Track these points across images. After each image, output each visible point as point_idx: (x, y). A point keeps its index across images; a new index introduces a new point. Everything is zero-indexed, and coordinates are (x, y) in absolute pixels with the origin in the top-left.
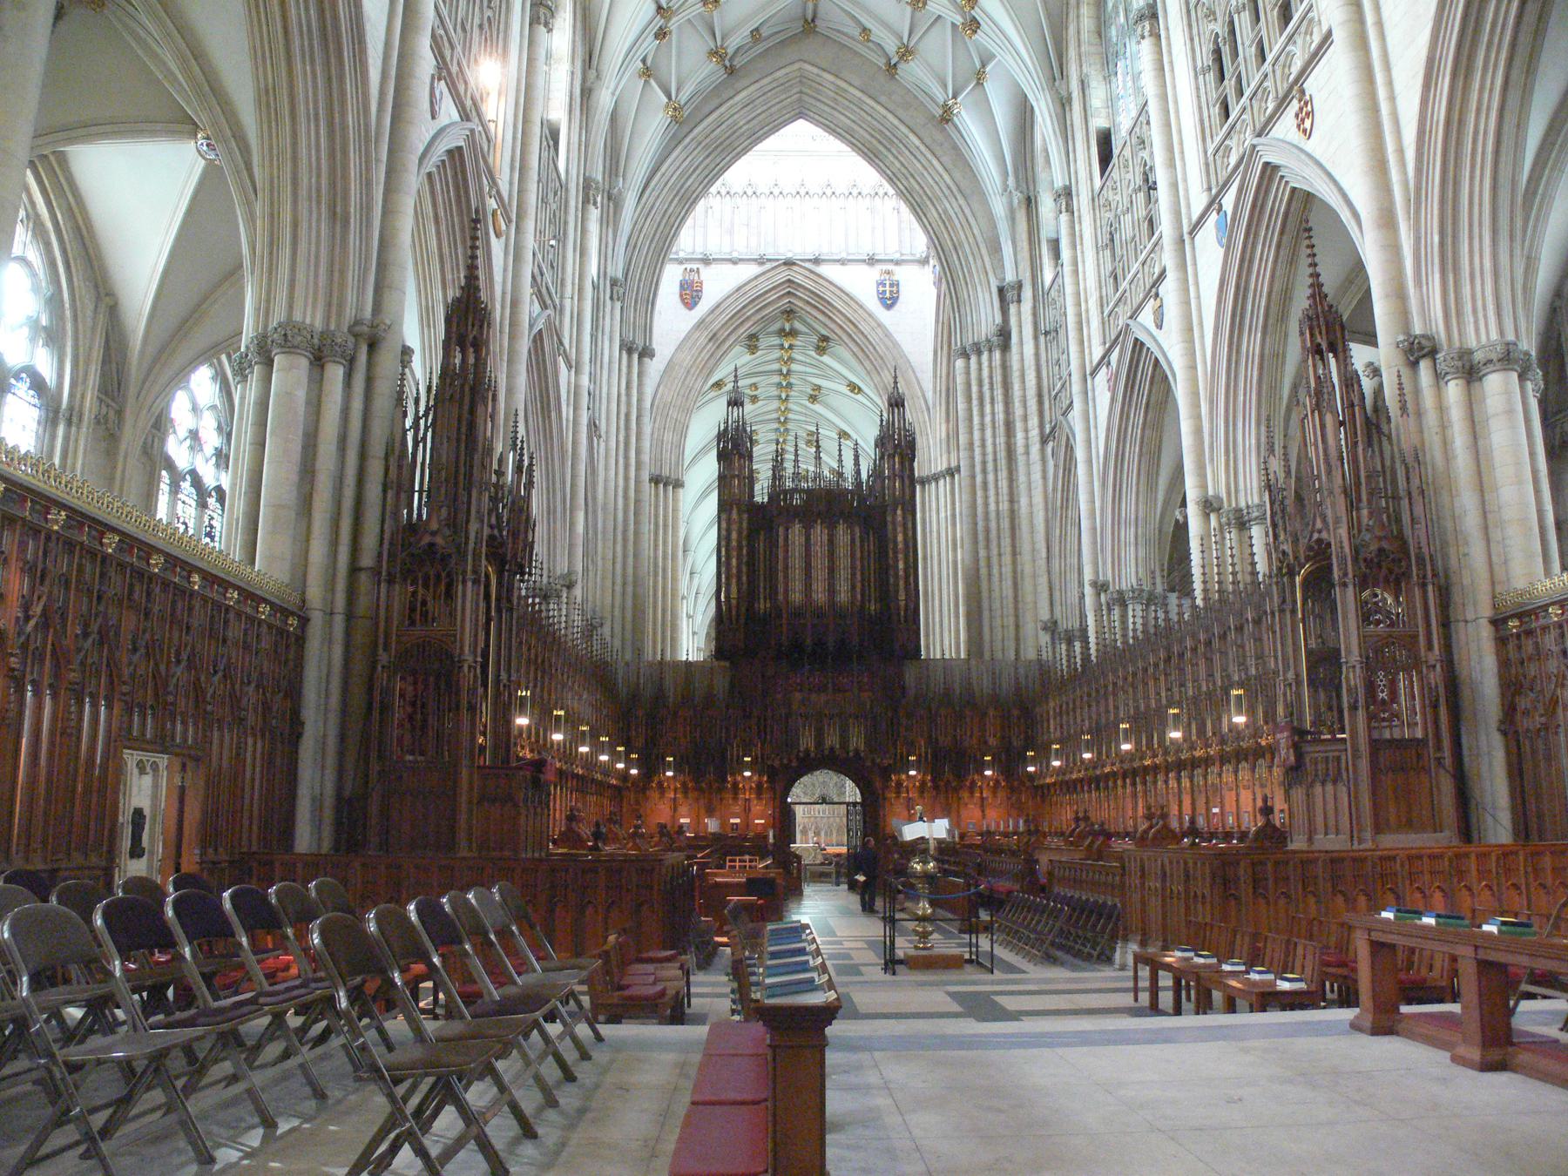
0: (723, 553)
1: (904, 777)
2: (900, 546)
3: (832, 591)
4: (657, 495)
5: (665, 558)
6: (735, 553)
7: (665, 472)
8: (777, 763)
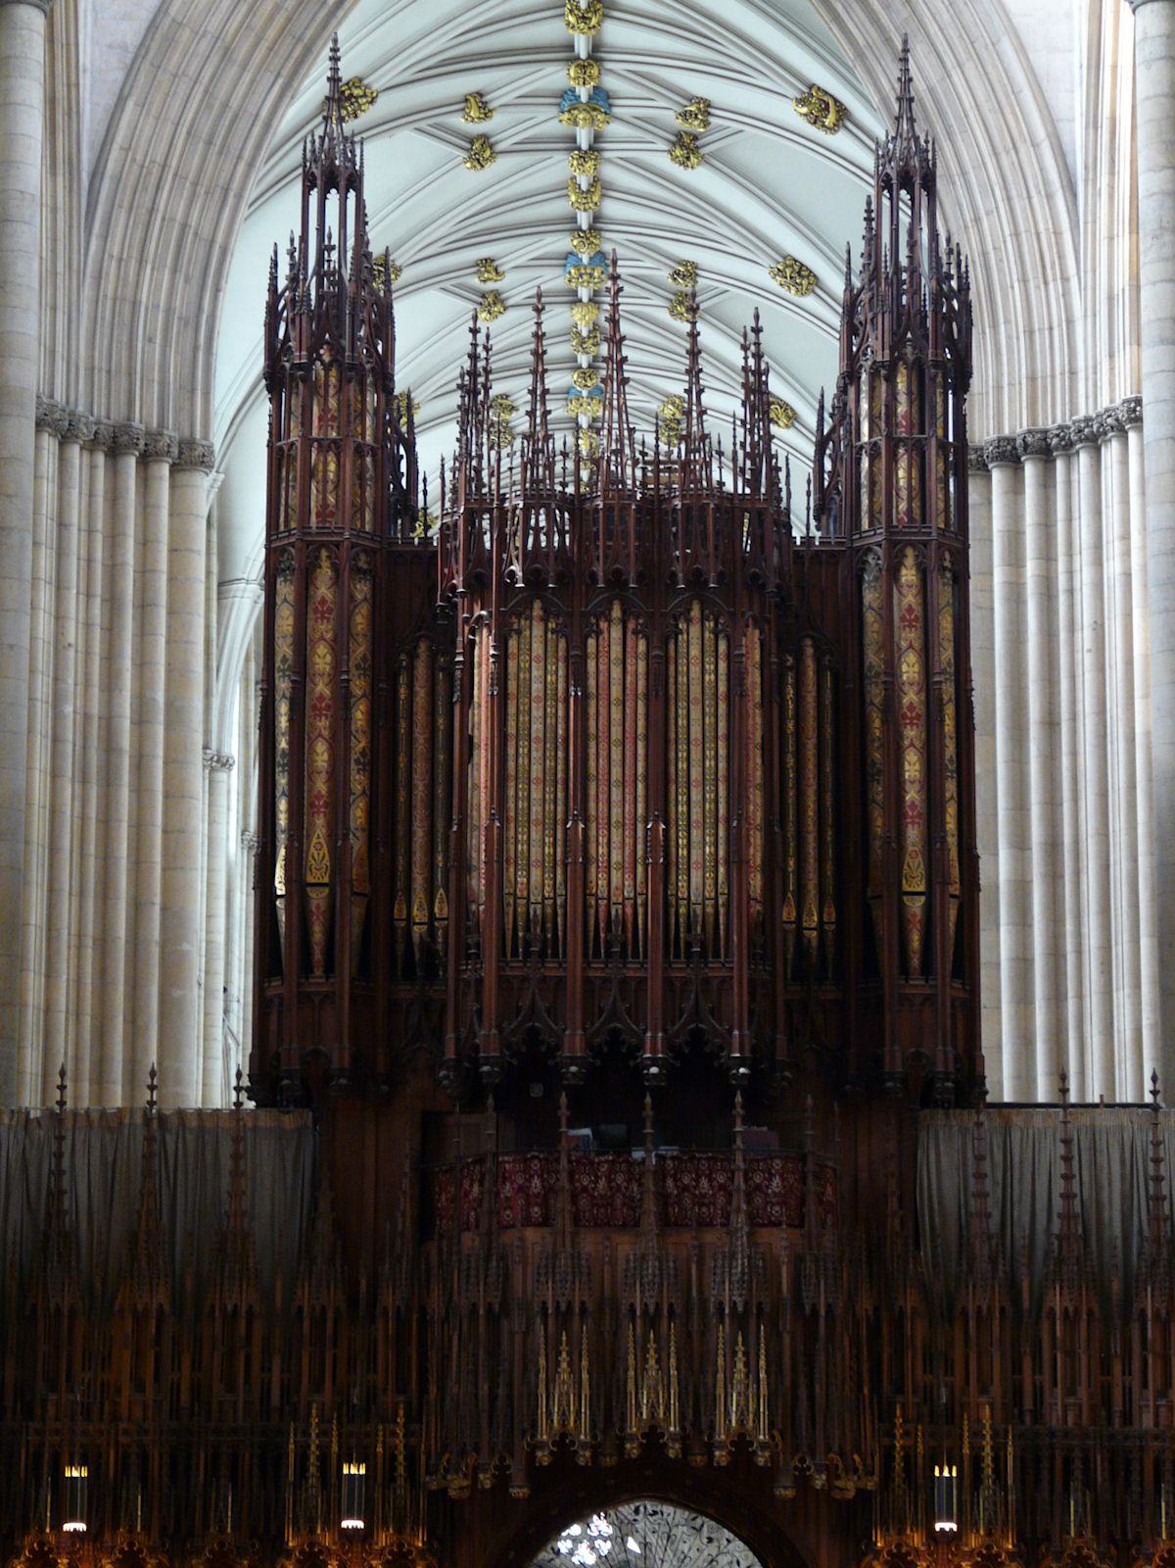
0: (283, 722)
1: (917, 1540)
2: (911, 697)
3: (663, 863)
4: (114, 498)
5: (141, 721)
6: (323, 724)
7: (145, 416)
8: (457, 1485)
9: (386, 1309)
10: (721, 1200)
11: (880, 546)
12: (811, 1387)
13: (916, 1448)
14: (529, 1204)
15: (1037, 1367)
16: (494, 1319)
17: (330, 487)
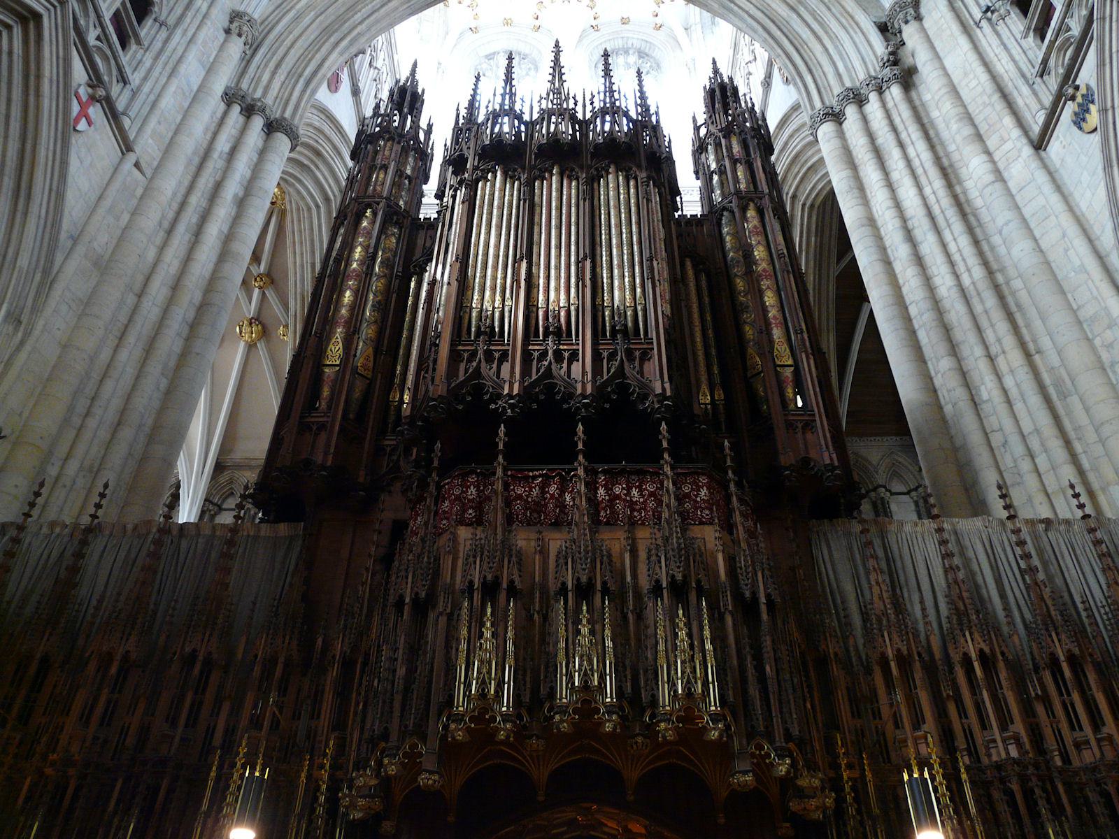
9: (334, 657)
10: (652, 504)
11: (731, 202)
12: (760, 669)
13: (863, 776)
14: (464, 511)
15: (963, 713)
16: (422, 608)
17: (379, 183)
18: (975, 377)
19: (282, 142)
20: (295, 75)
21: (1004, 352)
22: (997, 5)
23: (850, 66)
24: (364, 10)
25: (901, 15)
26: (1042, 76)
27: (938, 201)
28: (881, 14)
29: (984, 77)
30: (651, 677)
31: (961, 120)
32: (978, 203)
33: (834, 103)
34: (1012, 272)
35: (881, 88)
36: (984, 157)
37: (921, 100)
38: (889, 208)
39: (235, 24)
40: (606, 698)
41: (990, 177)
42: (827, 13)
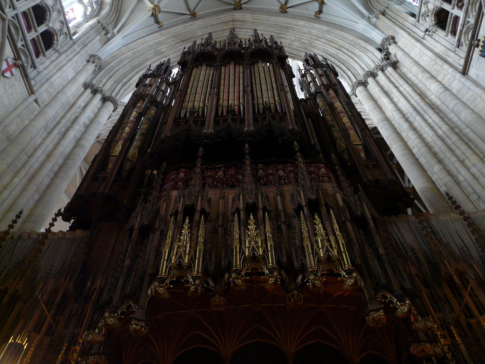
18: (454, 171)
19: (110, 106)
20: (118, 82)
21: (467, 158)
22: (430, 29)
23: (367, 64)
24: (150, 61)
25: (387, 43)
26: (458, 47)
27: (418, 104)
28: (377, 45)
29: (430, 54)
30: (300, 253)
31: (423, 72)
32: (439, 103)
33: (362, 79)
34: (463, 126)
35: (383, 69)
36: (438, 83)
37: (402, 72)
38: (394, 111)
39: (92, 59)
40: (269, 263)
41: (443, 90)
42: (354, 48)
